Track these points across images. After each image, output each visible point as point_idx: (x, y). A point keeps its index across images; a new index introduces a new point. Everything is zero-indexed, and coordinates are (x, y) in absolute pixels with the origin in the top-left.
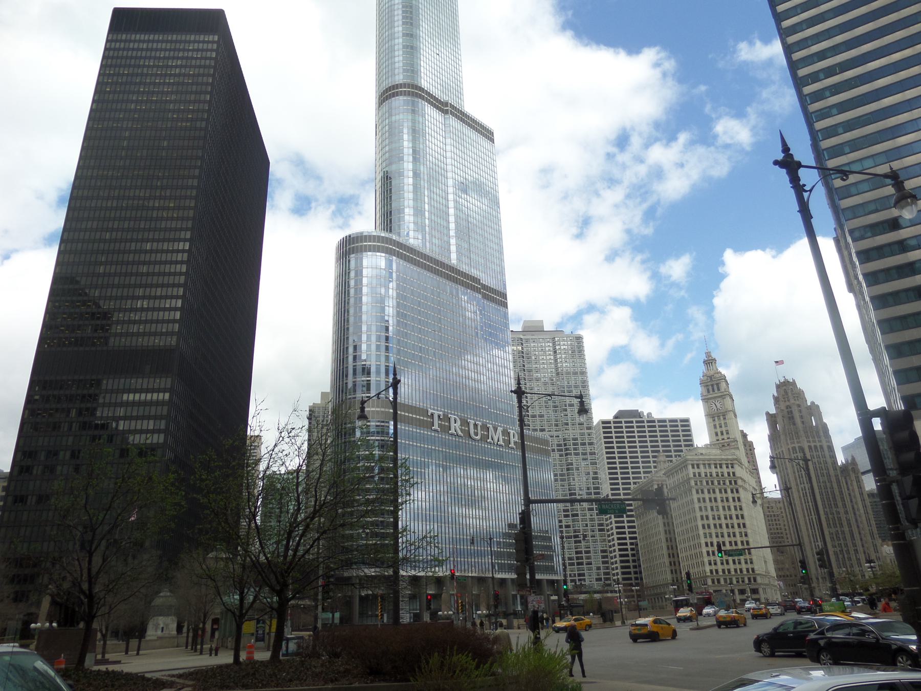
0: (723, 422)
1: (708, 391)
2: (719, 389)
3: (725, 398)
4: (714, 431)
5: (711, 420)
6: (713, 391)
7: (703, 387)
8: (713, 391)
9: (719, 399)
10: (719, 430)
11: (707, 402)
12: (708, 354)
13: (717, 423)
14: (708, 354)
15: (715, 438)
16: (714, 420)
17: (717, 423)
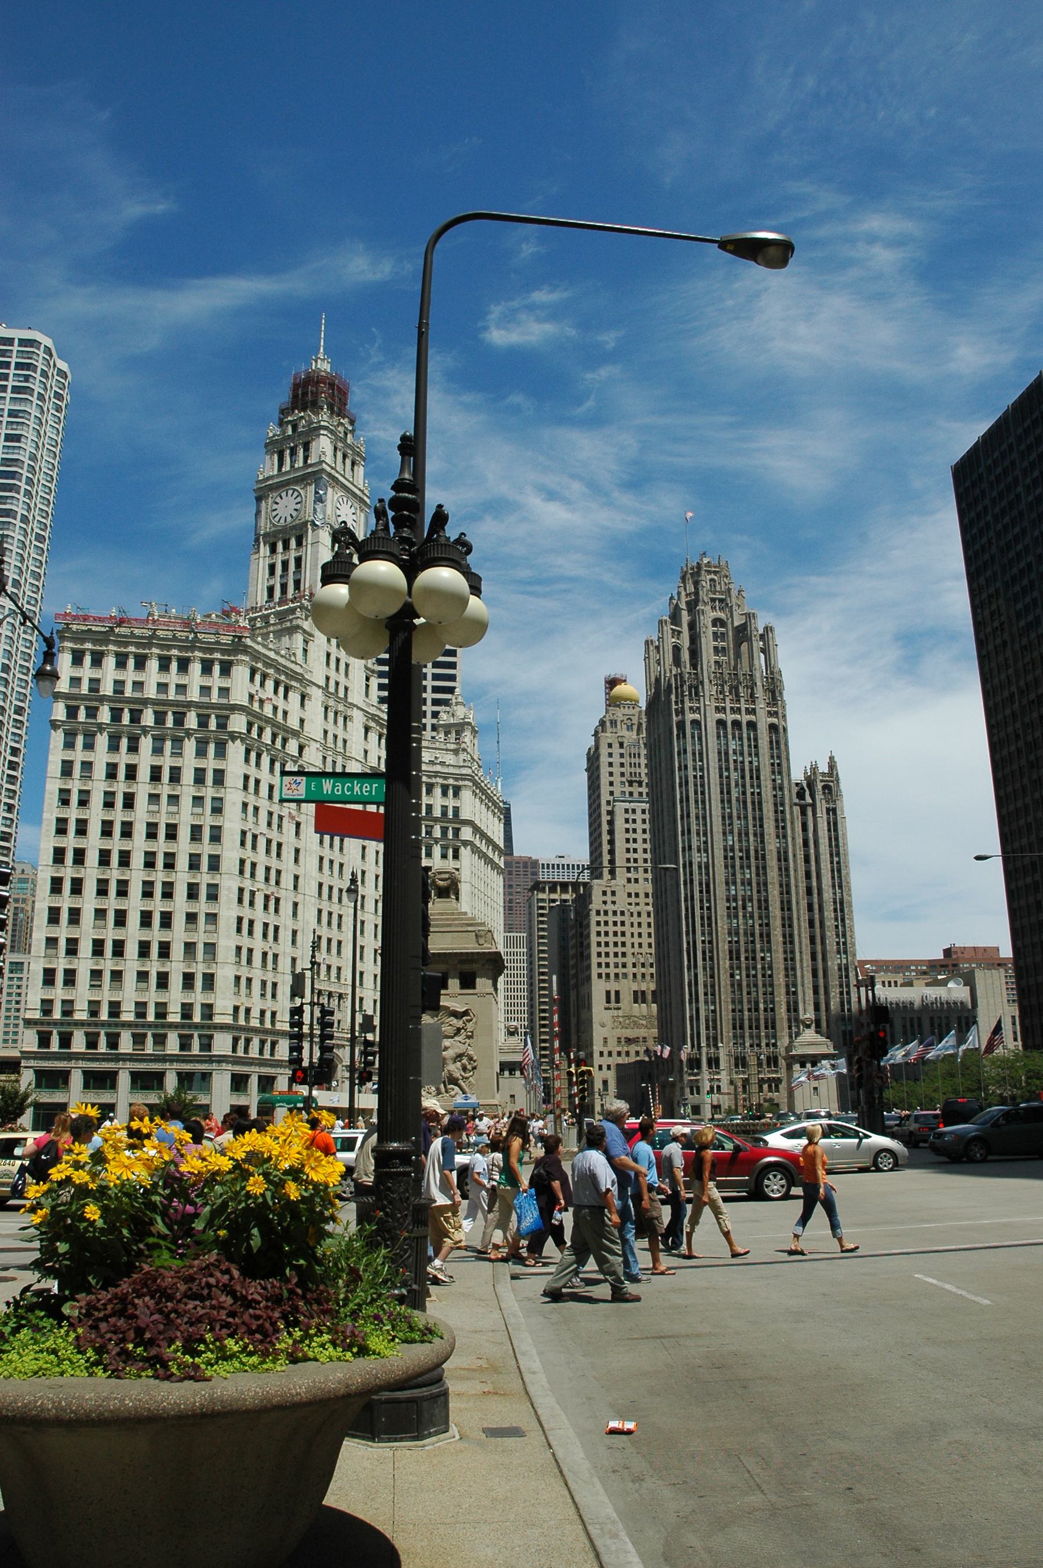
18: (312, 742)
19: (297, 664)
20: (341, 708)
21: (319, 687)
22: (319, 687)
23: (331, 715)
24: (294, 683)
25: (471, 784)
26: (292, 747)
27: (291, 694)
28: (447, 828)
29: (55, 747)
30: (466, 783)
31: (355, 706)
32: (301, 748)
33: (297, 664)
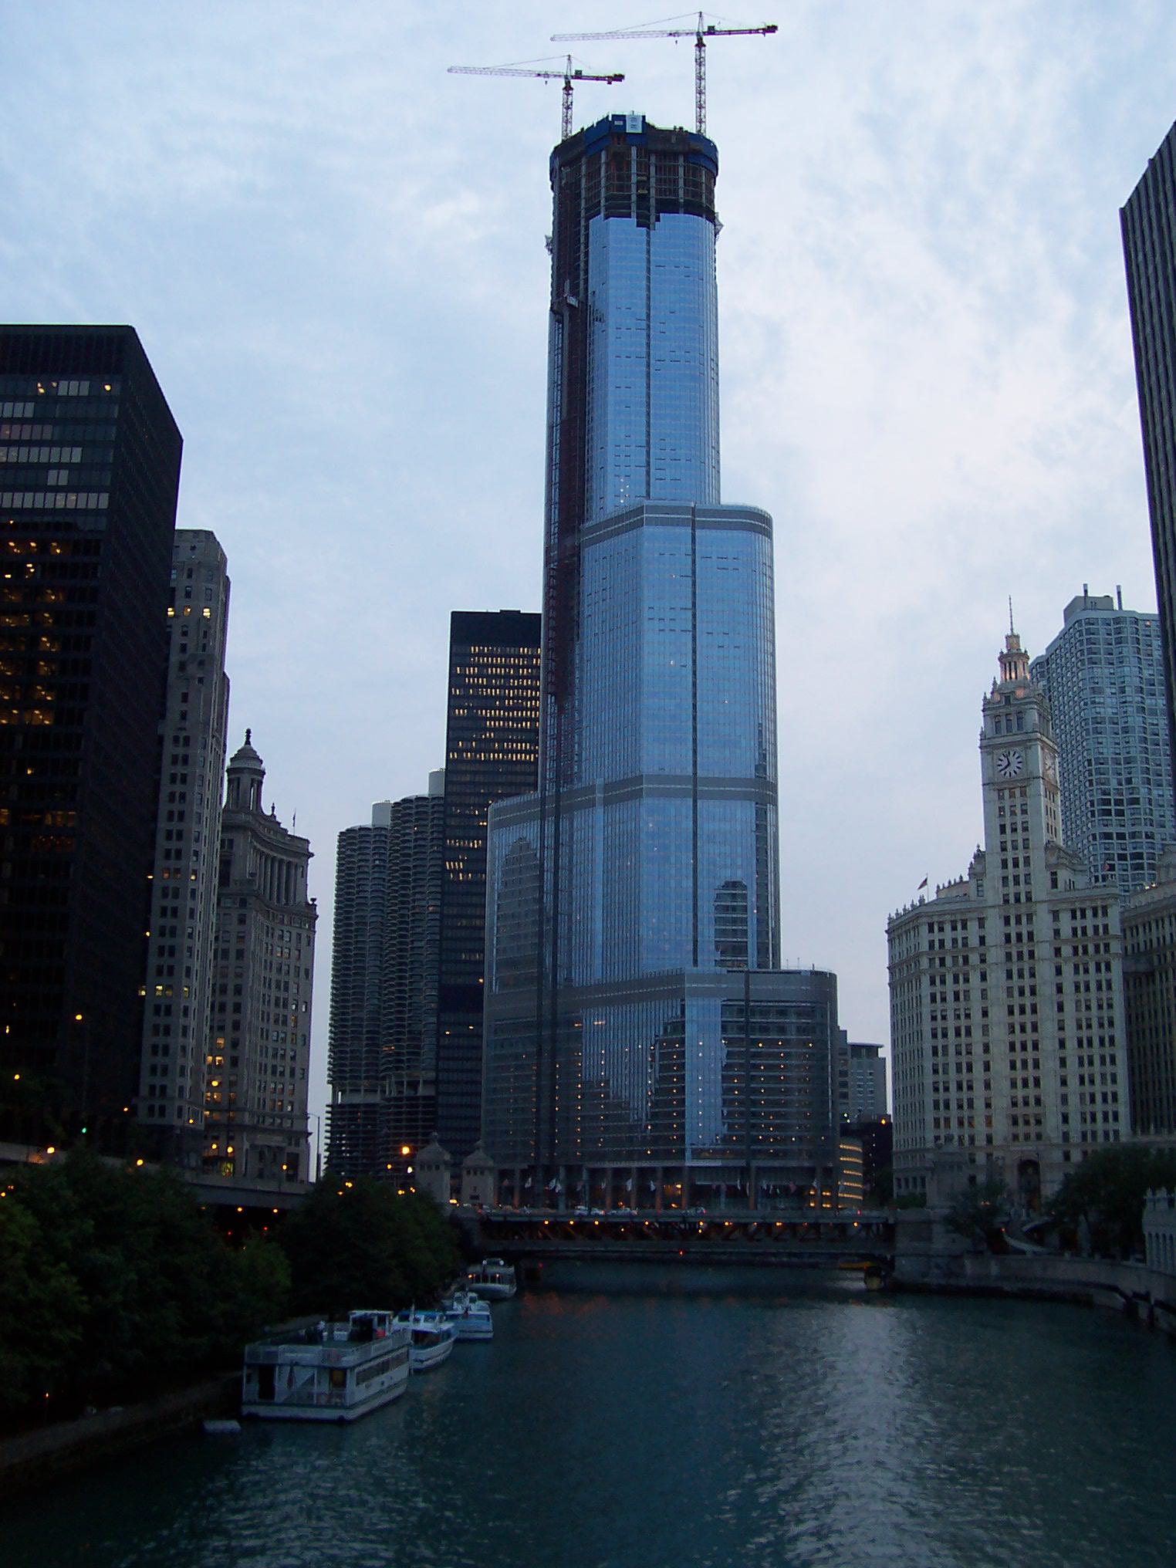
0: (1018, 801)
1: (998, 729)
2: (1020, 726)
3: (1030, 747)
4: (996, 823)
5: (995, 795)
6: (1009, 729)
7: (988, 717)
8: (1009, 729)
9: (1017, 749)
10: (1008, 821)
12: (1012, 639)
13: (1007, 804)
14: (1012, 639)
15: (997, 838)
16: (1001, 798)
17: (1007, 804)
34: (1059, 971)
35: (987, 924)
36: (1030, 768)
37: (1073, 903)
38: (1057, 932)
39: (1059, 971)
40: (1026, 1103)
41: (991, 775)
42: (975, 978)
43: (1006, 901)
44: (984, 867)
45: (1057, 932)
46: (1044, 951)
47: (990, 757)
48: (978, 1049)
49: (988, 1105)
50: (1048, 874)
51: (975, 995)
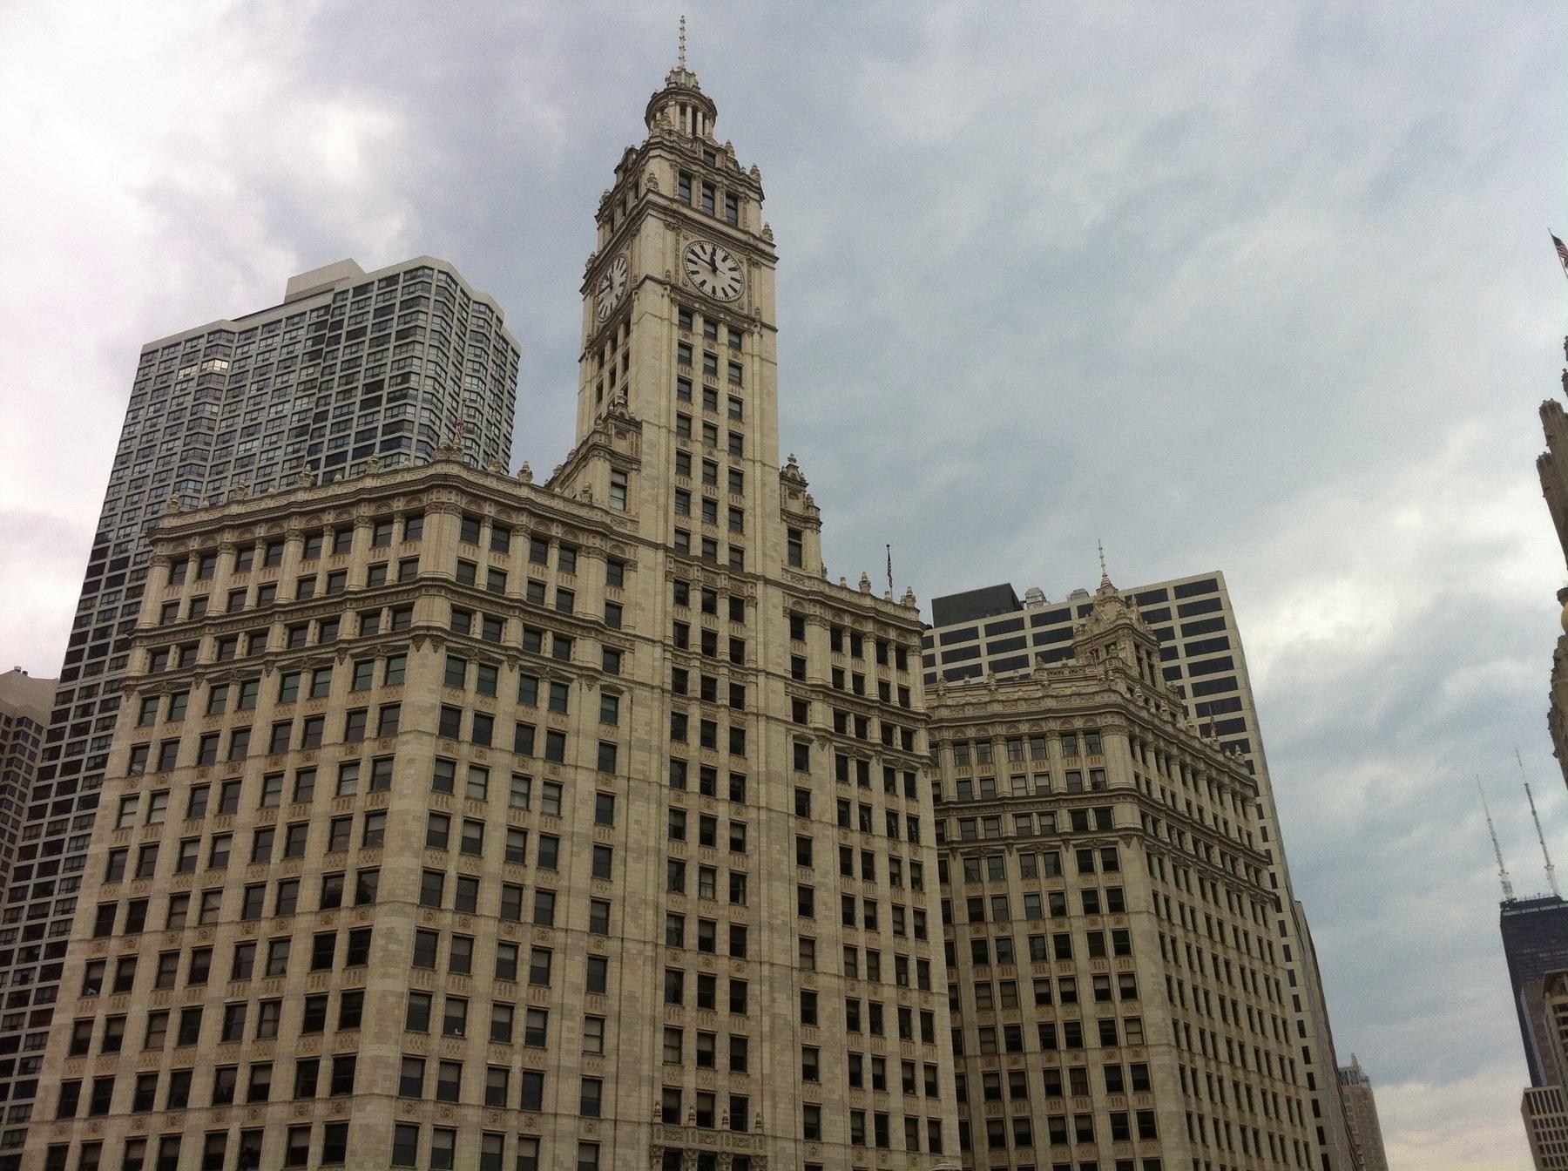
3: (756, 264)
9: (737, 256)
11: (668, 226)
18: (639, 645)
19: (591, 507)
20: (722, 582)
21: (656, 546)
22: (656, 546)
23: (696, 598)
24: (583, 540)
25: (1118, 721)
26: (587, 652)
27: (581, 562)
28: (1084, 812)
29: (124, 725)
30: (1109, 720)
31: (757, 578)
32: (613, 657)
33: (591, 507)
34: (801, 762)
35: (630, 579)
36: (756, 302)
37: (839, 612)
38: (799, 665)
39: (801, 762)
40: (705, 1119)
41: (670, 266)
42: (585, 703)
43: (683, 548)
44: (636, 447)
45: (799, 665)
46: (768, 696)
47: (670, 235)
48: (573, 913)
49: (590, 1107)
50: (784, 529)
51: (582, 750)
